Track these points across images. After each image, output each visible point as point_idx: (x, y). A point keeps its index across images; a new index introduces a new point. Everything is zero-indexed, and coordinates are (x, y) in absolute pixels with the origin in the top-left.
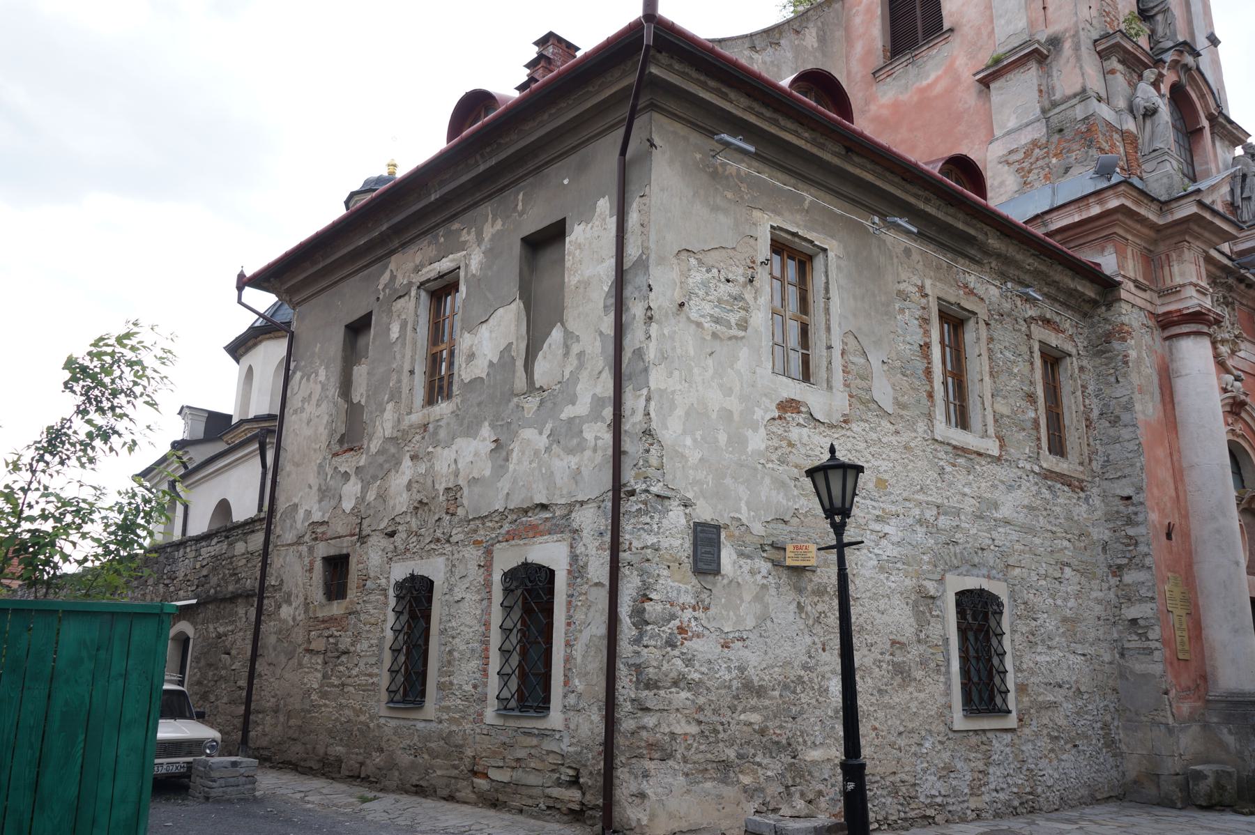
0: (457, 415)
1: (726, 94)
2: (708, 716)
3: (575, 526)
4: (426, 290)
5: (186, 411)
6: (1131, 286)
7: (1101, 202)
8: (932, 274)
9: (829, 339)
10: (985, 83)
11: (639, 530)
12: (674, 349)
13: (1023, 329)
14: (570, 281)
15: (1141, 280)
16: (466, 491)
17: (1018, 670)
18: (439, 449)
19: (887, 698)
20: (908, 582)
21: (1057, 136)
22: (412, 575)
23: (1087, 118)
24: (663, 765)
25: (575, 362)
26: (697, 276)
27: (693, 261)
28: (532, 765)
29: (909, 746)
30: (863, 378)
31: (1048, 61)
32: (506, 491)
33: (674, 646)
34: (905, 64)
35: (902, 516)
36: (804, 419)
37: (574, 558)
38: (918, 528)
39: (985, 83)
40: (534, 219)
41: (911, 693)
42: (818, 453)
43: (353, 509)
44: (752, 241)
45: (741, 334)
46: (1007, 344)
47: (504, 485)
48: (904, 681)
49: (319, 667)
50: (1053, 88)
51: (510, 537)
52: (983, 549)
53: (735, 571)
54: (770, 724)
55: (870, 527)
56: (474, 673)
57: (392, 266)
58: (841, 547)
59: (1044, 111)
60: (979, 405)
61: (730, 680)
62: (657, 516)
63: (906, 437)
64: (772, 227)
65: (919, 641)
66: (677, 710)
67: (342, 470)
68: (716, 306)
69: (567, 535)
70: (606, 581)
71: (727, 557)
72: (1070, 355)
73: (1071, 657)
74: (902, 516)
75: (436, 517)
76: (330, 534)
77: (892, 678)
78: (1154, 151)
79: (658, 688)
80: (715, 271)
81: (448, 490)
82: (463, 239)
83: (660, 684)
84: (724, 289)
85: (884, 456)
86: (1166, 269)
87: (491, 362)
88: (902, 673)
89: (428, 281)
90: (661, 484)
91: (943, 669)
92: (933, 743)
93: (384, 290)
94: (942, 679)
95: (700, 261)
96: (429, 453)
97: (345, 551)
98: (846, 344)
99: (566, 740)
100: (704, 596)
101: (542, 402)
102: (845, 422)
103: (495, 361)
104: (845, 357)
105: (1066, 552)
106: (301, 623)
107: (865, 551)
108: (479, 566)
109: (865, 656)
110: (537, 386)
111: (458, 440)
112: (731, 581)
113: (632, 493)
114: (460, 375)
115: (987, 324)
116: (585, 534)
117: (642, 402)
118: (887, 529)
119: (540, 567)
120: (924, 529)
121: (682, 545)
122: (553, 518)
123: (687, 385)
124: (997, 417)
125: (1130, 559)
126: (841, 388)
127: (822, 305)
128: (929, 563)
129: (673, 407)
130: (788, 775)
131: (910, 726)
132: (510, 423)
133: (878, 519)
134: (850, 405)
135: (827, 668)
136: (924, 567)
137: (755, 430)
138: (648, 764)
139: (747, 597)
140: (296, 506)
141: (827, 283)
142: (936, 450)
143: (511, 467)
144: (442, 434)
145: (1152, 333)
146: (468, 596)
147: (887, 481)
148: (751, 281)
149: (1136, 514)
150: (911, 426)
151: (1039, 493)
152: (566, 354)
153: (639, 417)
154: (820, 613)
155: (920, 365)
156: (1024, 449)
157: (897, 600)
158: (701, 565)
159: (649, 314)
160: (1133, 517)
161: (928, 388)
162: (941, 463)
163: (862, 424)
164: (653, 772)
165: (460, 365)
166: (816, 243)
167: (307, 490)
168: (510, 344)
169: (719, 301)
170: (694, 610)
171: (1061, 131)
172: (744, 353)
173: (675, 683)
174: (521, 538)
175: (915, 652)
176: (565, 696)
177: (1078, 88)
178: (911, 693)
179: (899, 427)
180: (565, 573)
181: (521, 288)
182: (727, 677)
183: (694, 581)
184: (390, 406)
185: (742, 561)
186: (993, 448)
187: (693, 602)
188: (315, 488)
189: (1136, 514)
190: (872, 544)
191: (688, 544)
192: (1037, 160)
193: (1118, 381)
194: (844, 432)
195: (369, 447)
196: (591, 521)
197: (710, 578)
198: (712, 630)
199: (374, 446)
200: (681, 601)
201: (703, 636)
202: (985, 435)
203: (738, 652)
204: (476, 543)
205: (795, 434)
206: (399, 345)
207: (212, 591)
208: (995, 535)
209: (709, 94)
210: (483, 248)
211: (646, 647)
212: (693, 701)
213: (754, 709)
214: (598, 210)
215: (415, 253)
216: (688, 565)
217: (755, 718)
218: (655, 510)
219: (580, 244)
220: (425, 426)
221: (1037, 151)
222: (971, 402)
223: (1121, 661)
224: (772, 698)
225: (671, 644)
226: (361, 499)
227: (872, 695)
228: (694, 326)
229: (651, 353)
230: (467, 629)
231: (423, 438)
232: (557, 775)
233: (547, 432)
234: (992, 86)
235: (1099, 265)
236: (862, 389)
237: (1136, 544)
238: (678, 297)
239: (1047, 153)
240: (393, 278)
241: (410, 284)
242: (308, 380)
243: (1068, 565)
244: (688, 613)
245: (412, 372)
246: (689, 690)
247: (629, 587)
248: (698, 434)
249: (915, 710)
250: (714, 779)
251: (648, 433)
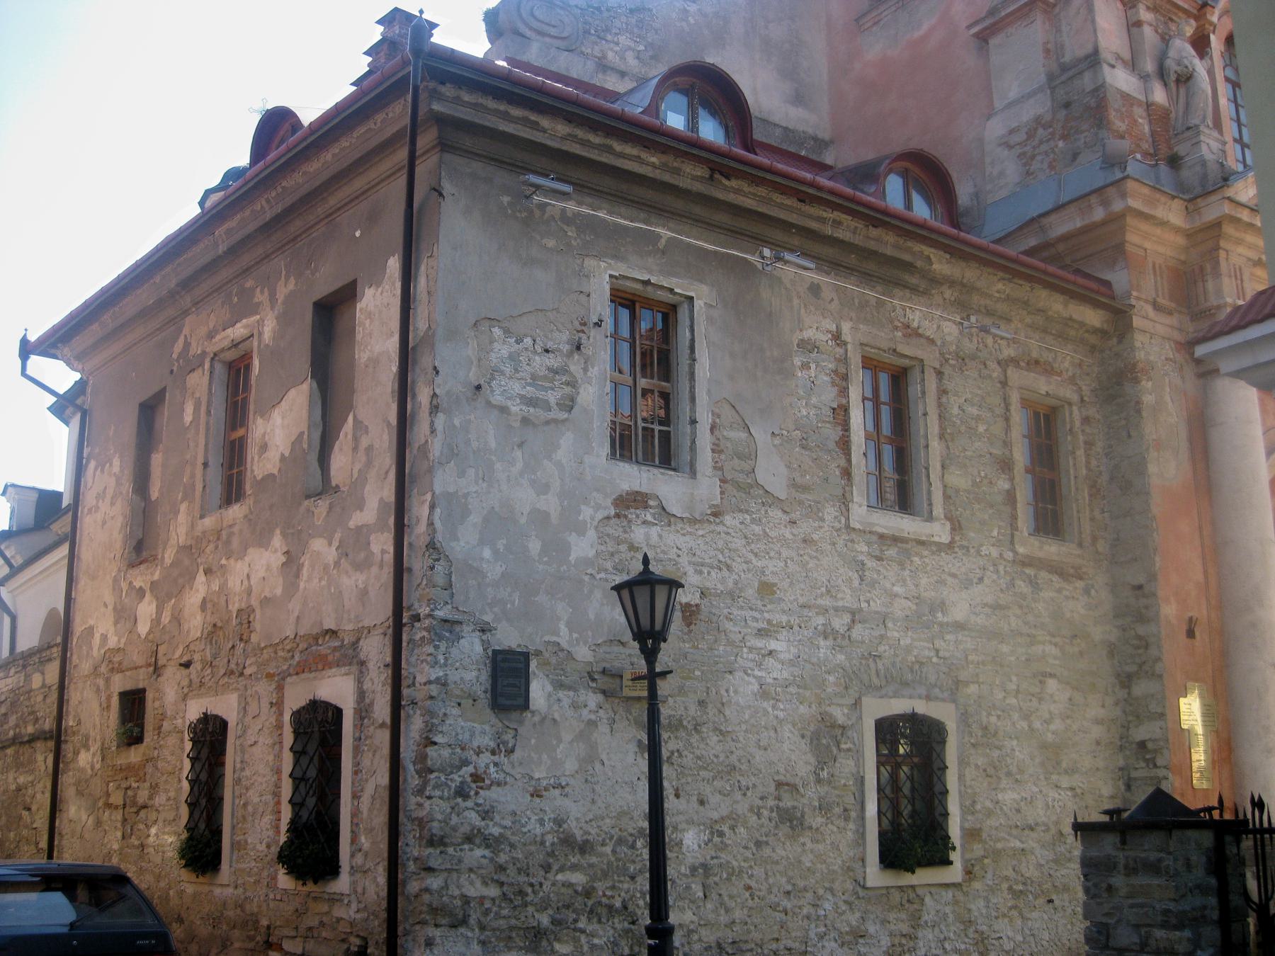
0: (250, 520)
1: (537, 123)
2: (512, 875)
3: (362, 656)
4: (224, 362)
5: (10, 489)
6: (1149, 310)
7: (1105, 203)
8: (853, 315)
9: (693, 410)
10: (983, 38)
11: (422, 662)
12: (468, 442)
13: (995, 375)
14: (360, 358)
15: (1159, 300)
16: (258, 612)
17: (967, 810)
18: (232, 561)
19: (767, 851)
20: (803, 709)
21: (1064, 112)
22: (205, 714)
23: (1096, 90)
24: (453, 932)
25: (364, 459)
26: (502, 349)
28: (324, 934)
29: (800, 908)
30: (741, 457)
31: (1057, 10)
32: (296, 614)
33: (466, 797)
34: (893, 8)
35: (796, 628)
36: (653, 515)
37: (361, 695)
38: (822, 643)
39: (983, 38)
40: (325, 282)
41: (804, 844)
42: (675, 557)
43: (148, 634)
44: (583, 298)
45: (565, 415)
46: (969, 396)
47: (295, 606)
48: (792, 828)
49: (119, 825)
50: (1062, 47)
51: (301, 669)
52: (922, 663)
53: (550, 707)
54: (598, 885)
55: (748, 644)
56: (267, 830)
57: (186, 331)
58: (652, 677)
59: (1051, 77)
60: (924, 479)
61: (543, 835)
62: (443, 645)
63: (805, 527)
64: (611, 276)
65: (819, 781)
66: (471, 870)
67: (137, 584)
68: (530, 385)
69: (354, 668)
70: (388, 721)
71: (539, 690)
72: (1070, 404)
73: (1053, 794)
74: (796, 628)
75: (230, 645)
76: (125, 664)
77: (776, 827)
78: (1188, 128)
79: (445, 845)
80: (528, 341)
81: (239, 611)
82: (256, 300)
83: (447, 840)
84: (541, 363)
85: (772, 554)
86: (1200, 284)
87: (282, 455)
88: (791, 821)
89: (223, 350)
90: (449, 607)
91: (853, 814)
92: (835, 904)
93: (178, 360)
94: (851, 826)
95: (507, 332)
96: (222, 566)
97: (141, 686)
98: (719, 416)
99: (354, 906)
100: (508, 737)
101: (331, 507)
102: (715, 515)
103: (287, 454)
104: (717, 432)
105: (1051, 661)
106: (99, 773)
107: (741, 674)
108: (271, 703)
109: (737, 802)
110: (334, 484)
111: (251, 550)
112: (543, 719)
113: (417, 618)
114: (252, 471)
115: (939, 374)
116: (371, 665)
117: (425, 511)
118: (773, 645)
119: (327, 705)
120: (830, 642)
121: (477, 678)
122: (342, 646)
123: (485, 485)
124: (949, 492)
125: (1140, 666)
126: (709, 471)
127: (687, 369)
128: (836, 684)
129: (466, 512)
130: (623, 943)
131: (801, 884)
132: (300, 532)
133: (761, 633)
134: (722, 493)
135: (681, 818)
136: (829, 690)
137: (581, 531)
138: (431, 931)
139: (567, 737)
140: (91, 630)
141: (693, 341)
142: (852, 541)
143: (302, 585)
144: (235, 543)
145: (1181, 369)
146: (261, 740)
147: (775, 585)
148: (578, 348)
149: (1147, 607)
150: (814, 512)
151: (1012, 584)
152: (355, 449)
153: (422, 528)
154: (672, 753)
155: (833, 433)
156: (992, 531)
157: (787, 731)
158: (501, 701)
159: (434, 402)
160: (1143, 611)
161: (843, 463)
162: (860, 558)
163: (740, 516)
164: (438, 940)
165: (253, 458)
166: (677, 290)
167: (103, 609)
168: (302, 433)
169: (534, 377)
170: (493, 753)
171: (1067, 105)
172: (567, 441)
173: (469, 839)
174: (310, 671)
175: (812, 794)
176: (352, 856)
177: (1089, 48)
178: (804, 844)
179: (795, 515)
180: (352, 711)
181: (314, 364)
182: (538, 831)
183: (494, 720)
184: (183, 507)
185: (561, 694)
186: (940, 531)
187: (492, 744)
188: (110, 607)
189: (1147, 607)
190: (751, 665)
191: (485, 676)
192: (1041, 142)
193: (1129, 436)
194: (712, 527)
195: (163, 557)
196: (376, 650)
197: (515, 715)
198: (518, 776)
199: (169, 556)
200: (475, 744)
201: (506, 783)
202: (930, 518)
203: (555, 802)
204: (270, 676)
205: (639, 534)
206: (193, 431)
207: (11, 733)
208: (939, 643)
209: (512, 125)
210: (276, 312)
211: (429, 798)
212: (492, 860)
213: (574, 868)
214: (388, 271)
215: (209, 315)
216: (484, 700)
217: (578, 878)
218: (441, 638)
219: (370, 313)
220: (219, 532)
221: (1040, 131)
222: (914, 475)
223: (1128, 795)
224: (601, 855)
225: (462, 793)
226: (156, 621)
227: (746, 848)
228: (496, 412)
229: (436, 448)
230: (260, 779)
231: (217, 547)
232: (345, 946)
233: (336, 544)
234: (994, 42)
235: (1108, 284)
236: (742, 471)
237: (1147, 647)
238: (473, 376)
239: (1053, 134)
240: (187, 345)
241: (204, 353)
242: (102, 471)
243: (1052, 675)
244: (486, 758)
245: (205, 465)
246: (488, 846)
247: (414, 728)
248: (501, 545)
249: (808, 864)
250: (521, 949)
251: (432, 546)
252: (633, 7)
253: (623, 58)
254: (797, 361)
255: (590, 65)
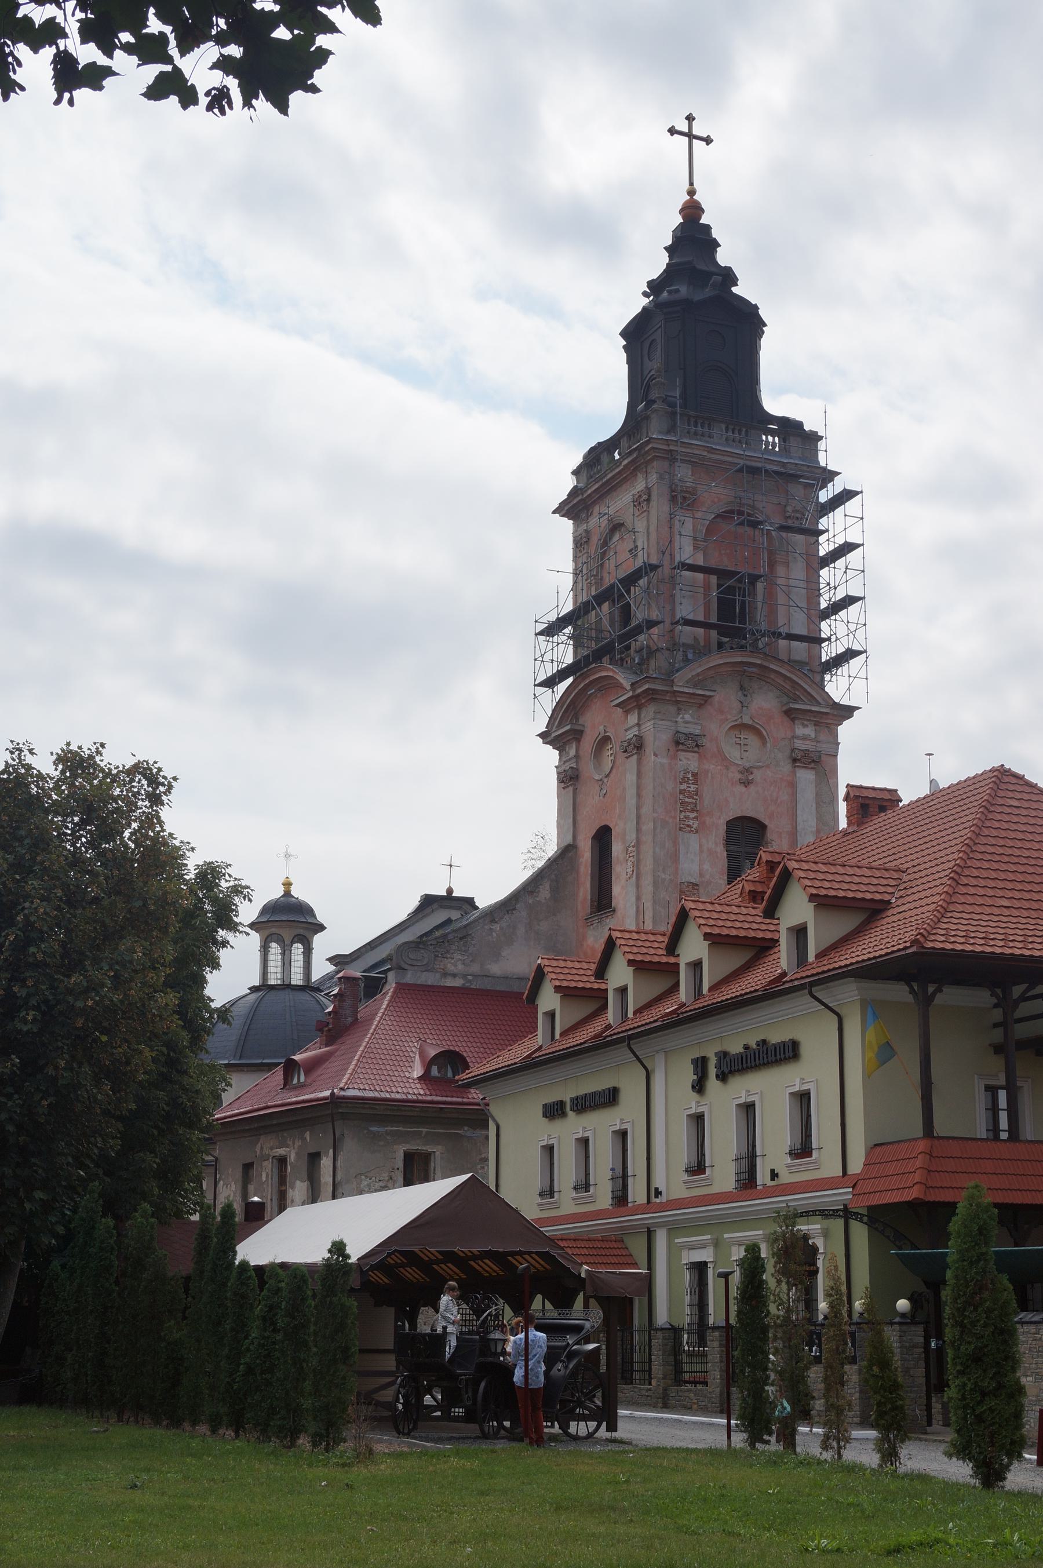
27: (363, 1177)
44: (393, 1160)
57: (261, 1141)
95: (366, 1177)
242: (227, 1187)
245: (271, 1200)
252: (461, 936)
253: (456, 966)
254: (479, 1167)
255: (438, 975)
